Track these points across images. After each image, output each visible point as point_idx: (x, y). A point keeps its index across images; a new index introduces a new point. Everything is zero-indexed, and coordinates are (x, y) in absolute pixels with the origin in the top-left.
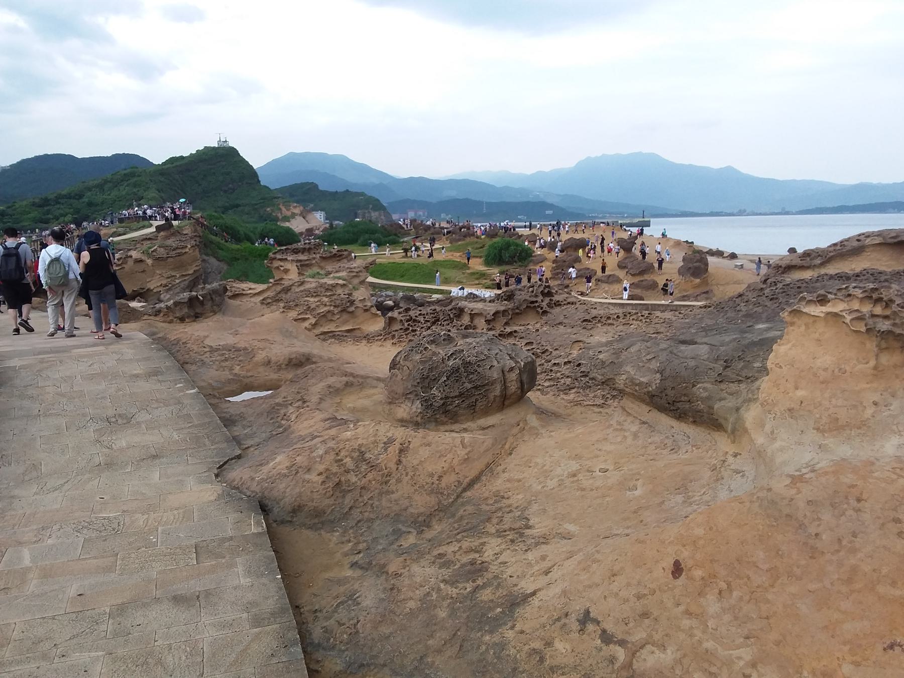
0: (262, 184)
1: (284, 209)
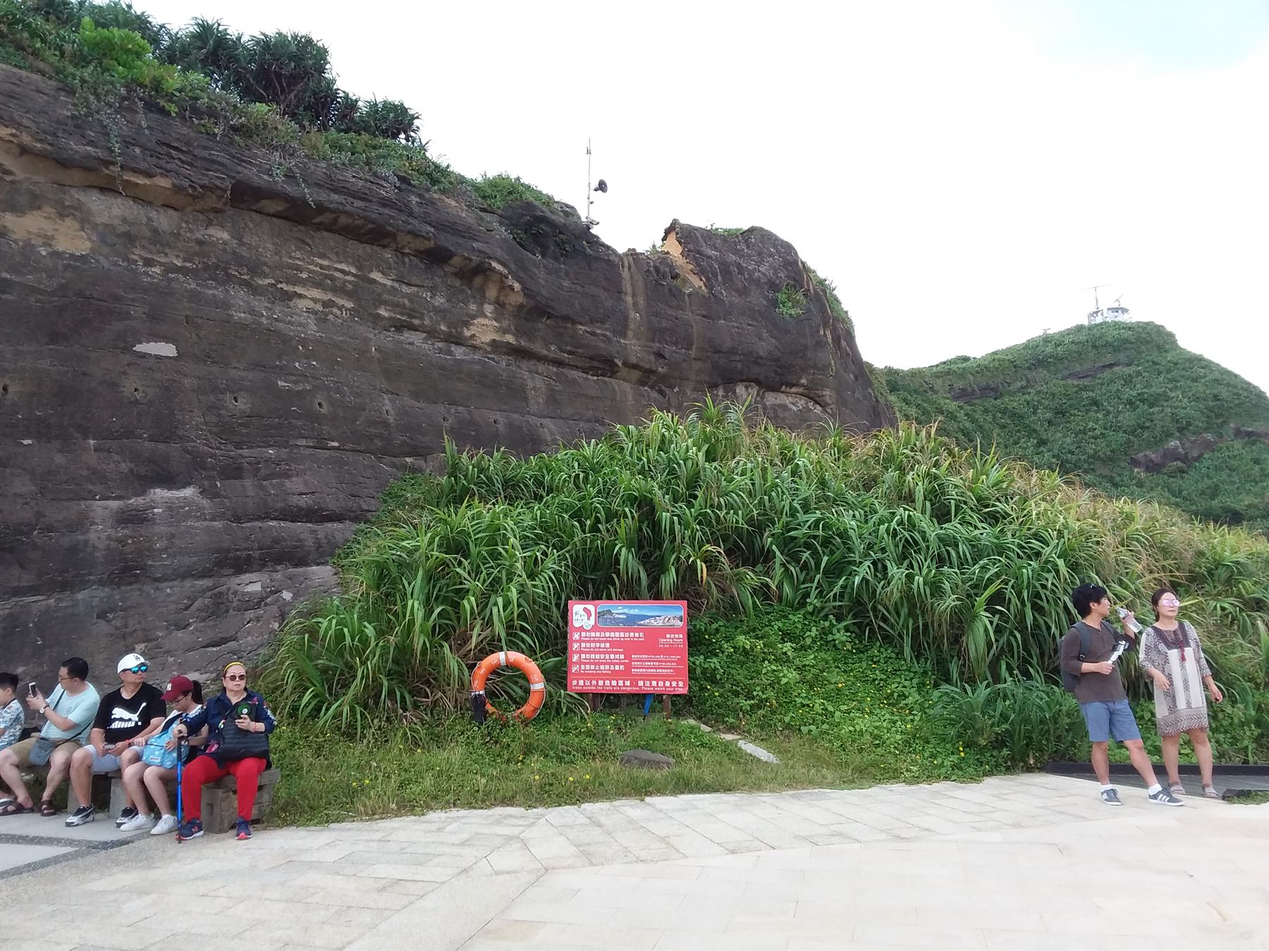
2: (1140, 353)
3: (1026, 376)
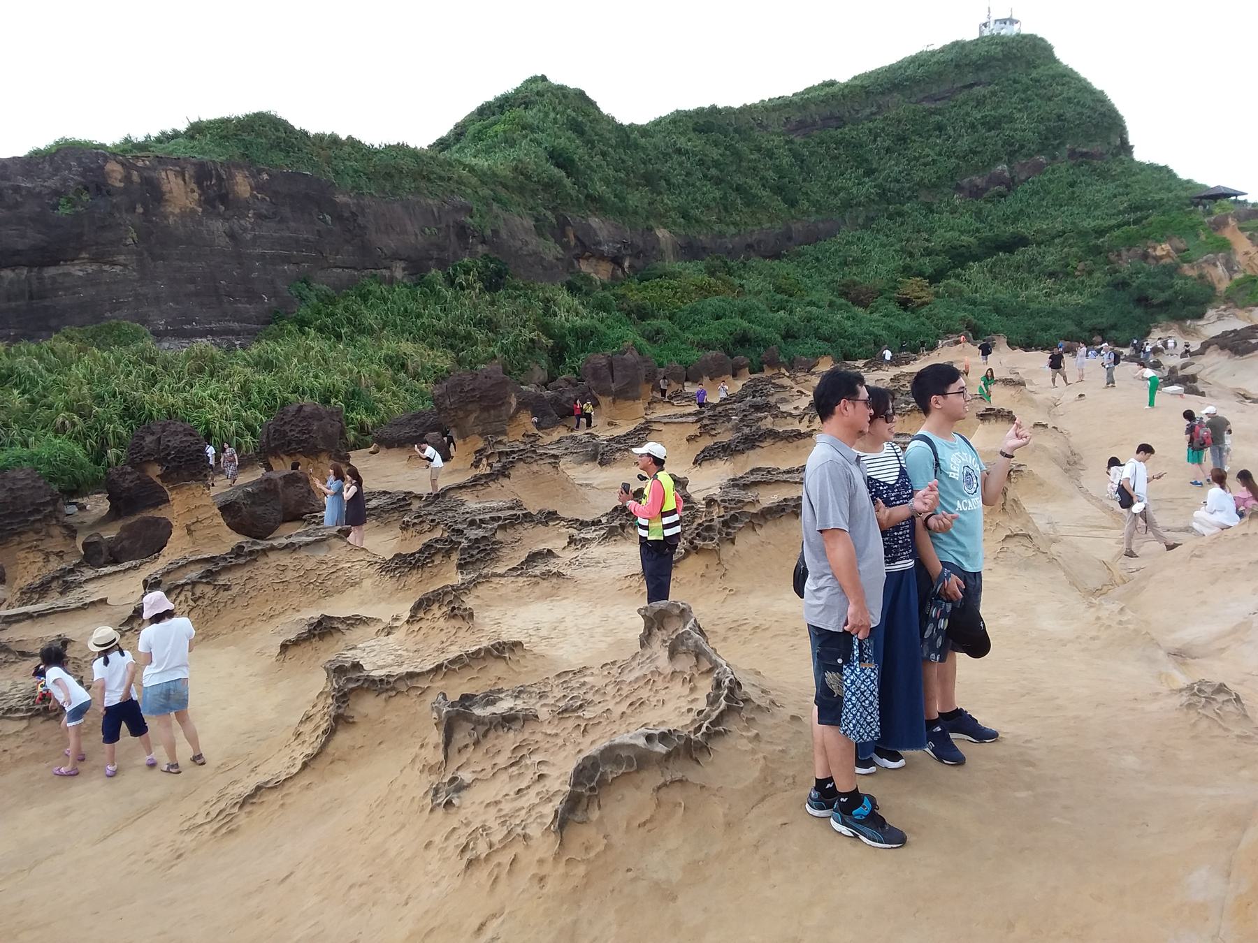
0: (1142, 154)
1: (1242, 244)
2: (1006, 70)
3: (876, 101)
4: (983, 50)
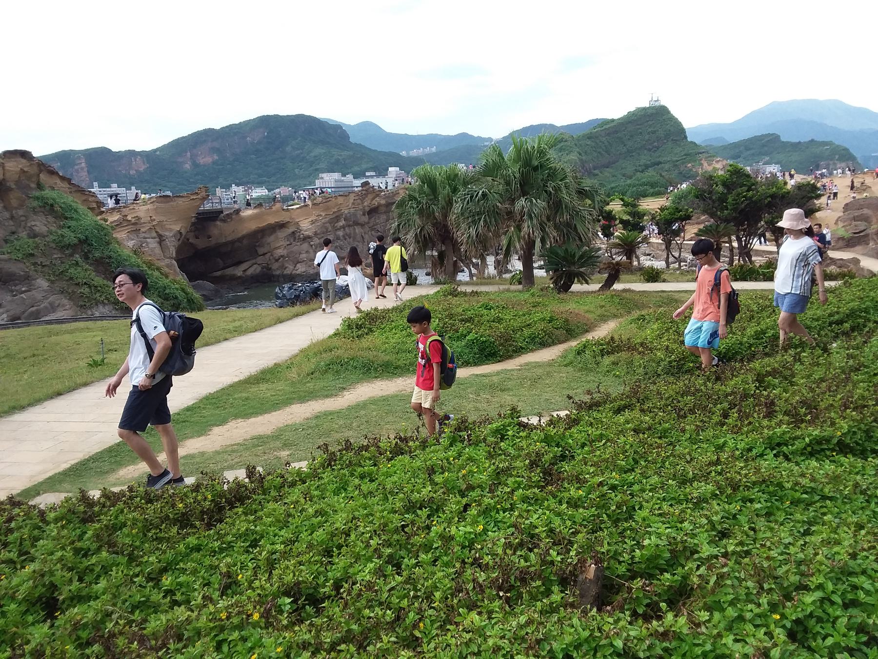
0: (689, 139)
1: (705, 164)
4: (650, 111)
